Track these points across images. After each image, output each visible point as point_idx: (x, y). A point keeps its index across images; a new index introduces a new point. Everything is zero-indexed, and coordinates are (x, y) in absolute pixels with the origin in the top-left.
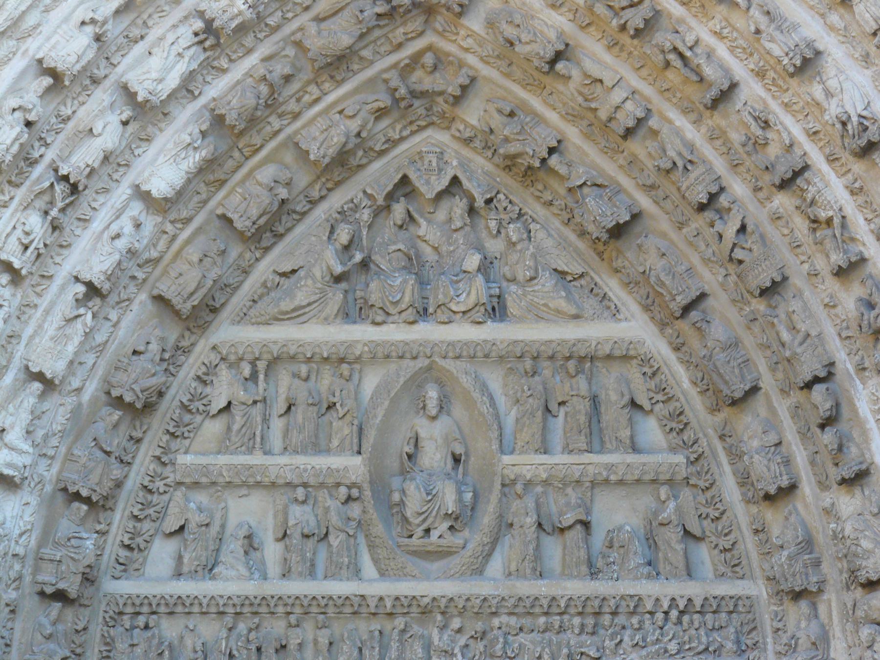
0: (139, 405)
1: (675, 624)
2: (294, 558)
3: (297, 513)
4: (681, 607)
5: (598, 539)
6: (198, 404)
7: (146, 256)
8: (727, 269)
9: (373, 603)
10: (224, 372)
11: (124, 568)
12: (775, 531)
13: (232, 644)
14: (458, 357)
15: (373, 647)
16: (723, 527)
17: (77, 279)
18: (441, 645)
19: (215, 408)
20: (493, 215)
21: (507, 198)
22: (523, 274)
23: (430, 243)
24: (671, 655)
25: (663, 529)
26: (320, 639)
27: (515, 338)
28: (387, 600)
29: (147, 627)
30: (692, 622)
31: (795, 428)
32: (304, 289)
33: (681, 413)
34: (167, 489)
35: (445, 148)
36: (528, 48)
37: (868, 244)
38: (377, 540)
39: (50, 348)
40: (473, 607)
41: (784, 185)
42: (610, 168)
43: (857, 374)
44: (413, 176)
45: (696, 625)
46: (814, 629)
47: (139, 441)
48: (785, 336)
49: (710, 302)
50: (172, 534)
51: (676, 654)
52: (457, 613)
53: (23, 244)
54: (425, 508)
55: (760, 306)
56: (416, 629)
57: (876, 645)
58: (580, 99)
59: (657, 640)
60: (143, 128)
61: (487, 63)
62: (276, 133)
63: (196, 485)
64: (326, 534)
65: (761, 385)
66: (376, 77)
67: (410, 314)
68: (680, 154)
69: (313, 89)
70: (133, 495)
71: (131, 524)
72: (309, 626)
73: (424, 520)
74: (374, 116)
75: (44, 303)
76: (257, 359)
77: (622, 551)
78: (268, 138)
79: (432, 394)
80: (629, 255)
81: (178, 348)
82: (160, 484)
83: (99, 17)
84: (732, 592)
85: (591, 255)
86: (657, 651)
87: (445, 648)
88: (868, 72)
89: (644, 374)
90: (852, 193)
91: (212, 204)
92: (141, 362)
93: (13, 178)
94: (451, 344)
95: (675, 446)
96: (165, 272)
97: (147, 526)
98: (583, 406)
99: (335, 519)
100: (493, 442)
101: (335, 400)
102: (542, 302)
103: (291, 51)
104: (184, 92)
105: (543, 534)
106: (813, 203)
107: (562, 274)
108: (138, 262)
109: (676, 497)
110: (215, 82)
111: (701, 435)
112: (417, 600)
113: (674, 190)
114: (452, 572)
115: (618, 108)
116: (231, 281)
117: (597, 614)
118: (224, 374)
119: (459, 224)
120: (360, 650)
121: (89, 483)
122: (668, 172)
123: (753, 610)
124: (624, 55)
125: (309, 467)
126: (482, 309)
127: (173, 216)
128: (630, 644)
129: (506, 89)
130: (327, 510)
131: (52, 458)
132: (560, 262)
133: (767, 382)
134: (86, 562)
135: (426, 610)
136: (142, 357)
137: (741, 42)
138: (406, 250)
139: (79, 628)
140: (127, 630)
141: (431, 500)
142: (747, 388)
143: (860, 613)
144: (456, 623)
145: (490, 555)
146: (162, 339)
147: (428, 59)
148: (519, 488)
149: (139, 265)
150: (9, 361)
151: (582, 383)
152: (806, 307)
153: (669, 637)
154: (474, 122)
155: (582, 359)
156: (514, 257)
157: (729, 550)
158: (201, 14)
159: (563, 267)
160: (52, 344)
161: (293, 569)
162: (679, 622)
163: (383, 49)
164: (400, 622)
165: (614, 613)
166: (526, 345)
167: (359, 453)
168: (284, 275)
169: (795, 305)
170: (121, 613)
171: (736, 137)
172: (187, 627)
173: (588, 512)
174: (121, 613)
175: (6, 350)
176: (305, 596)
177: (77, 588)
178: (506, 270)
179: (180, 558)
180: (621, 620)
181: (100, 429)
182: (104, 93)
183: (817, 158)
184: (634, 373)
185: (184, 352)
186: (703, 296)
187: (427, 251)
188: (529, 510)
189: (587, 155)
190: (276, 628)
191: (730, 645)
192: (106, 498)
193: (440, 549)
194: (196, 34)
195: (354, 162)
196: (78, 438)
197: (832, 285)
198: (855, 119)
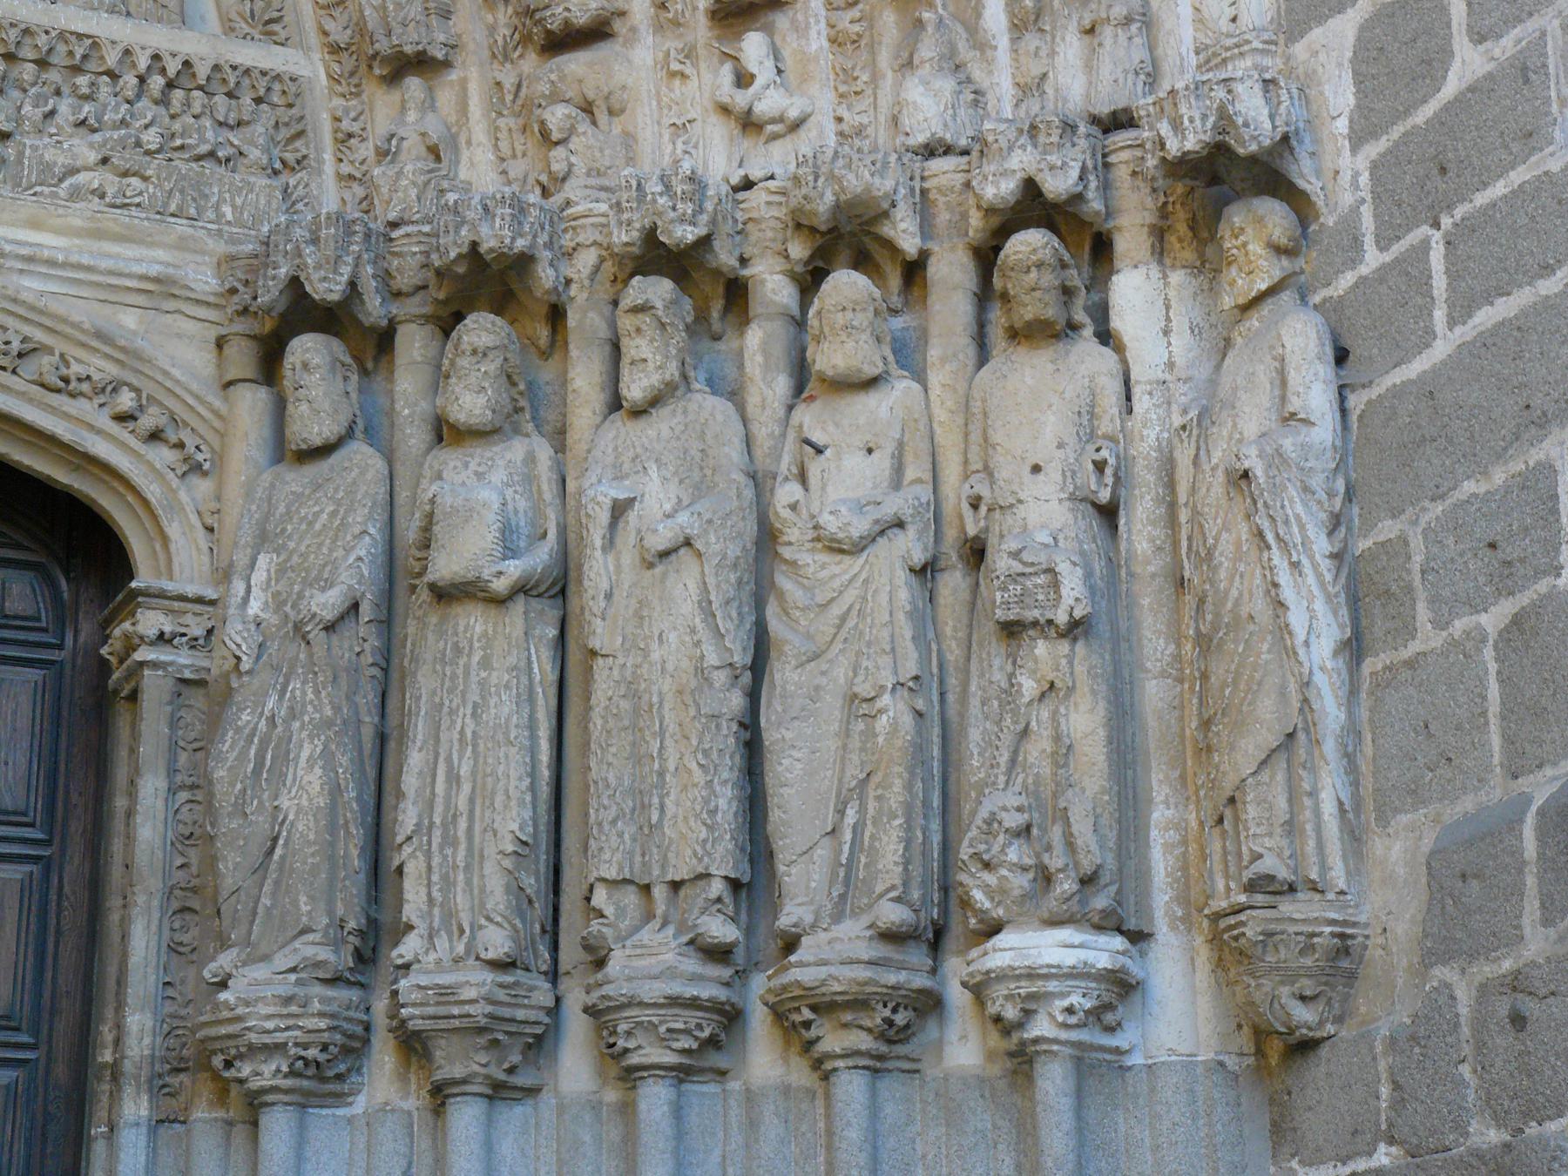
1: (156, 103)
4: (171, 72)
24: (148, 153)
30: (187, 104)
45: (197, 109)
51: (158, 151)
57: (574, 139)
59: (123, 121)
84: (265, 64)
86: (121, 139)
123: (298, 102)
128: (71, 118)
153: (146, 121)
180: (53, 76)
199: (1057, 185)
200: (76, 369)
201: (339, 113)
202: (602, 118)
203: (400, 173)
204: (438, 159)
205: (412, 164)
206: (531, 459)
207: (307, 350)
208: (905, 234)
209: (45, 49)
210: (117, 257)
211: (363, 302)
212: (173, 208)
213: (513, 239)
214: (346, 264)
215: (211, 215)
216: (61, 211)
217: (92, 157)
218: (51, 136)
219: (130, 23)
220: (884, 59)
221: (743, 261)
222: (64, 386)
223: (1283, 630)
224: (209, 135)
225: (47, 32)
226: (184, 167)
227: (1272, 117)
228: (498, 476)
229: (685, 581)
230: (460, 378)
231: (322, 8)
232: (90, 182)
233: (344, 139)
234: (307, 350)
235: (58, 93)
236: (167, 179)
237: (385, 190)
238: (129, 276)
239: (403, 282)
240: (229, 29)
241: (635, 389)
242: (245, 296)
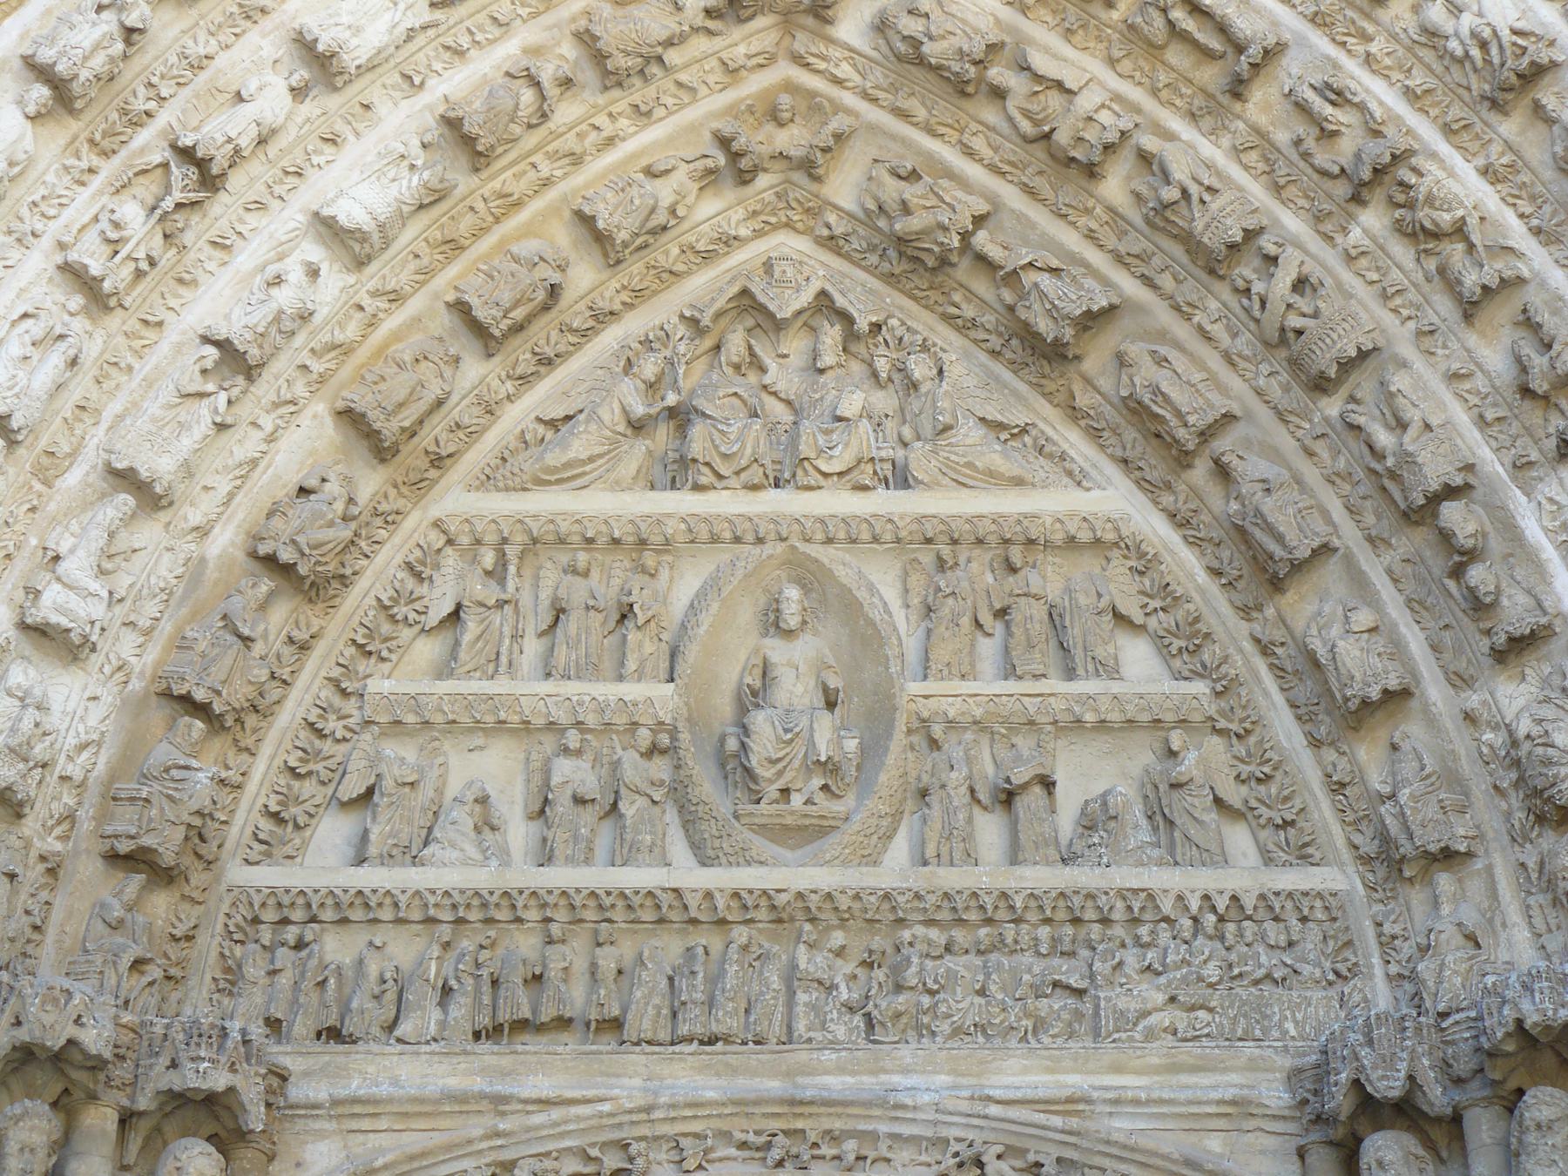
1: (1211, 938)
3: (564, 769)
8: (1271, 365)
10: (451, 562)
11: (265, 849)
12: (1377, 781)
13: (448, 969)
14: (829, 541)
15: (693, 973)
16: (1282, 788)
17: (206, 340)
18: (811, 969)
19: (433, 618)
21: (903, 323)
23: (782, 395)
24: (1211, 986)
25: (1176, 795)
26: (600, 962)
27: (922, 511)
28: (717, 895)
29: (300, 945)
31: (1401, 599)
32: (584, 436)
33: (1197, 620)
34: (348, 735)
35: (806, 259)
37: (1528, 253)
38: (700, 808)
39: (151, 433)
40: (866, 911)
42: (1072, 240)
43: (1514, 479)
47: (304, 647)
51: (1218, 983)
52: (836, 922)
53: (109, 241)
54: (780, 754)
58: (1026, 126)
61: (875, 100)
62: (547, 183)
64: (615, 805)
65: (1336, 542)
66: (701, 125)
70: (290, 735)
73: (780, 774)
74: (696, 186)
75: (144, 368)
76: (505, 541)
77: (1113, 824)
78: (531, 193)
84: (1305, 886)
86: (1184, 979)
87: (819, 975)
89: (1131, 569)
93: (98, 137)
95: (1187, 674)
97: (308, 788)
98: (1039, 611)
100: (892, 663)
101: (631, 599)
102: (963, 461)
104: (397, 78)
105: (977, 810)
106: (1430, 200)
108: (312, 344)
109: (1199, 747)
110: (446, 74)
111: (1231, 651)
112: (770, 898)
113: (1178, 251)
114: (828, 856)
116: (466, 421)
118: (450, 559)
120: (671, 979)
121: (209, 679)
125: (587, 698)
126: (869, 469)
129: (905, 142)
130: (616, 765)
132: (989, 408)
133: (1349, 535)
134: (194, 805)
135: (784, 916)
136: (312, 497)
138: (745, 395)
139: (178, 933)
140: (264, 947)
141: (792, 740)
142: (1315, 544)
145: (889, 836)
146: (347, 480)
149: (312, 350)
151: (1034, 580)
154: (848, 203)
156: (915, 404)
157: (1292, 823)
159: (993, 414)
161: (557, 852)
166: (943, 522)
167: (672, 680)
168: (552, 424)
170: (256, 921)
172: (371, 943)
175: (71, 429)
176: (578, 890)
177: (176, 849)
180: (1118, 931)
182: (264, 36)
185: (387, 522)
186: (1229, 418)
188: (954, 762)
189: (1033, 226)
193: (807, 822)
198: (1505, 34)
201: (1380, 919)
203: (1442, 964)
204: (1478, 946)
205: (1455, 956)
207: (1379, 1149)
209: (1106, 909)
210: (1195, 1087)
211: (1424, 1093)
212: (1240, 1033)
213: (1555, 1010)
214: (1401, 1060)
215: (1275, 1034)
216: (1139, 1053)
217: (1160, 998)
218: (1121, 985)
219: (1177, 871)
224: (1263, 959)
225: (1106, 893)
226: (1243, 994)
230: (1528, 1154)
231: (1349, 824)
232: (1162, 1021)
233: (1387, 943)
234: (1379, 1149)
235: (1123, 945)
236: (1231, 1006)
237: (1430, 983)
238: (1208, 1103)
239: (1463, 1067)
240: (1268, 859)
242: (1315, 1104)
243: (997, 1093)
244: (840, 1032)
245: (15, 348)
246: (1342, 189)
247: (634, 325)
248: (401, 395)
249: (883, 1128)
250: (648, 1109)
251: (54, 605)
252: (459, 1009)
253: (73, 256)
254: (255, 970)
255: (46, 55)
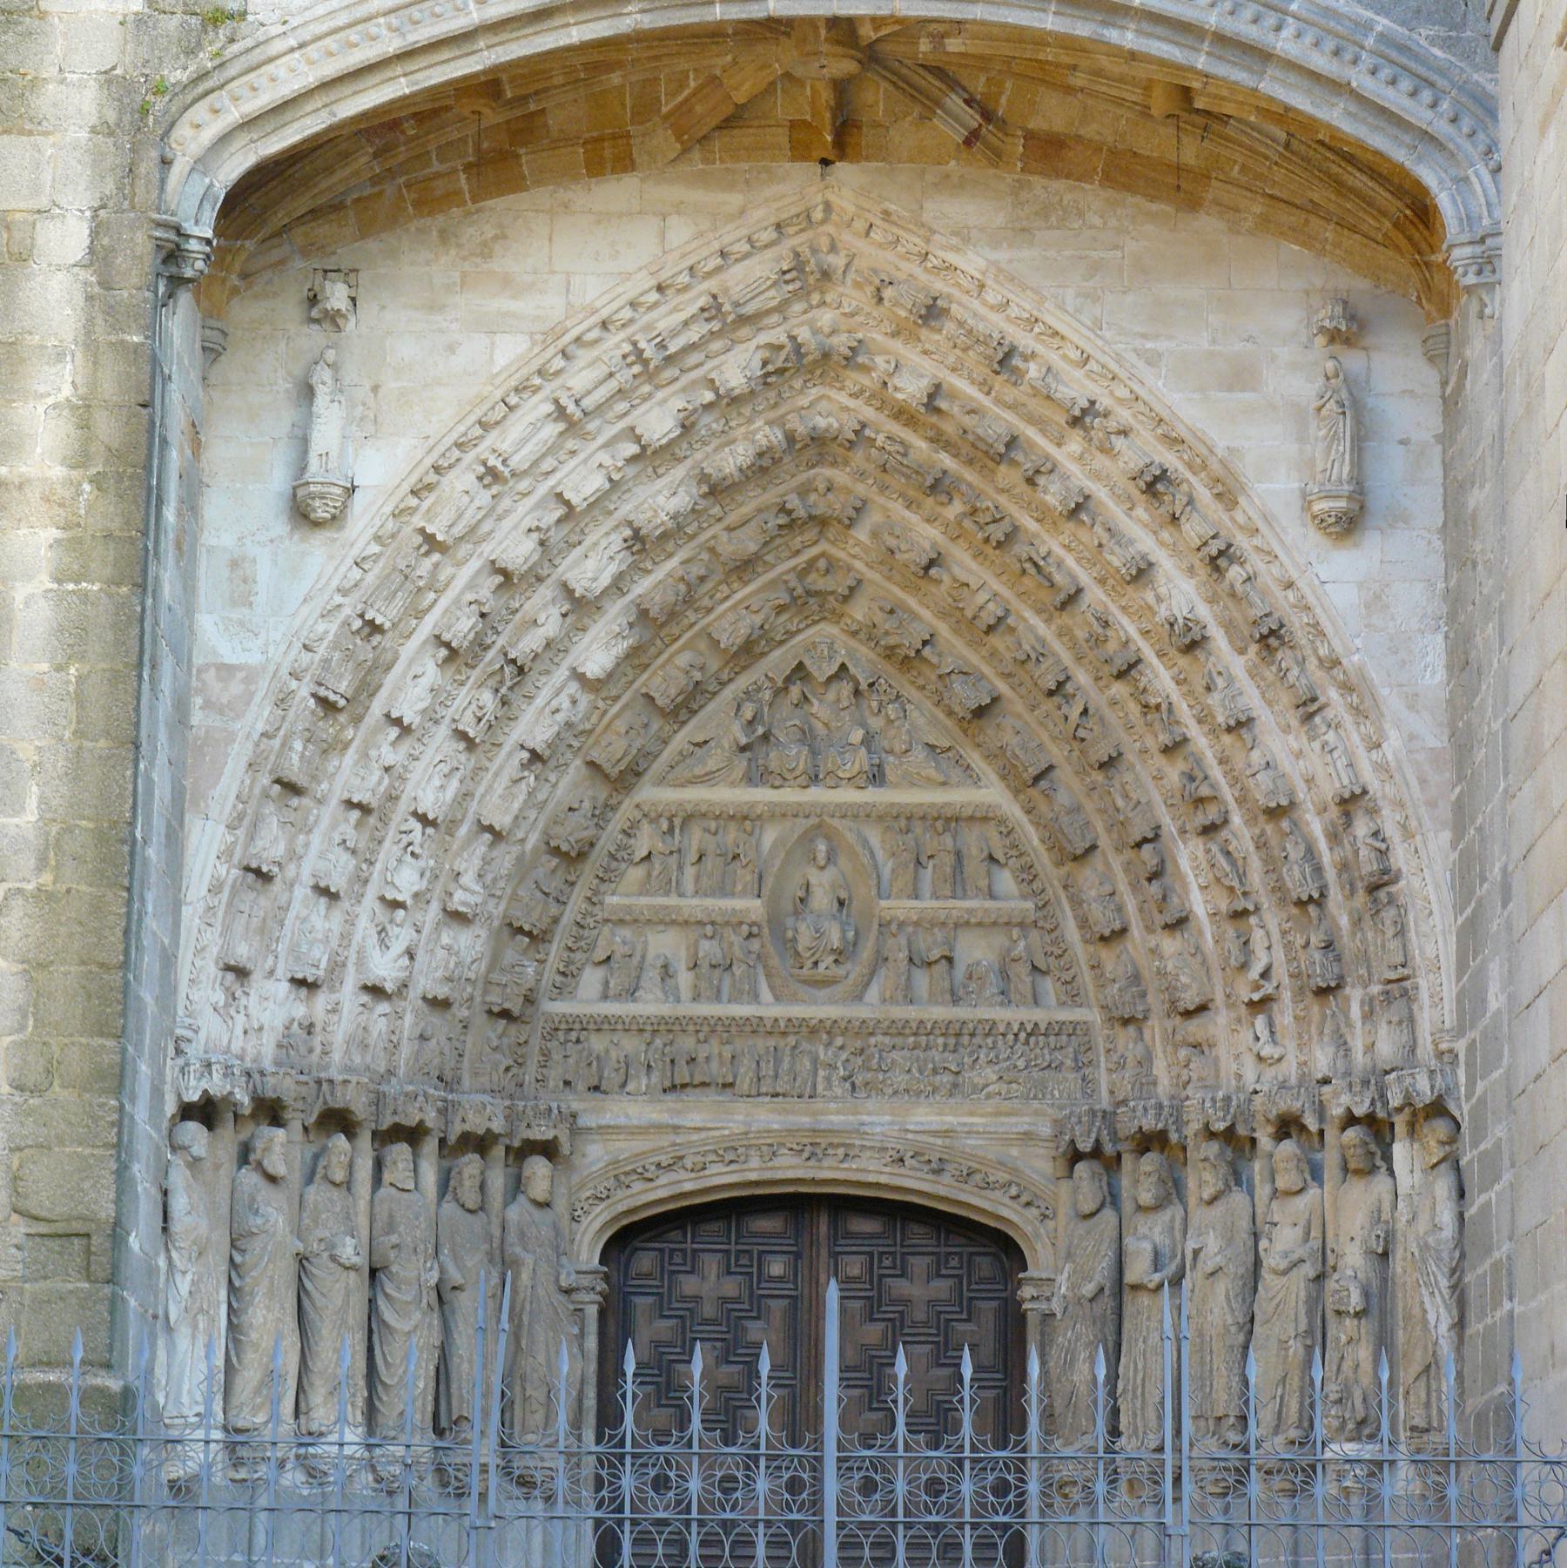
0: (573, 854)
2: (703, 985)
3: (706, 946)
5: (960, 971)
6: (623, 854)
7: (581, 727)
9: (769, 1024)
11: (560, 991)
14: (843, 817)
17: (522, 747)
20: (875, 696)
22: (899, 747)
36: (906, 556)
41: (1121, 675)
42: (974, 659)
44: (807, 662)
46: (1139, 1050)
47: (573, 884)
48: (1120, 803)
49: (1056, 773)
50: (600, 963)
55: (1099, 777)
56: (805, 1046)
60: (580, 619)
62: (692, 625)
63: (622, 922)
67: (803, 780)
68: (1033, 648)
69: (724, 587)
71: (565, 954)
72: (714, 1042)
75: (494, 767)
79: (822, 847)
80: (989, 732)
81: (607, 805)
82: (590, 921)
83: (543, 525)
85: (957, 731)
88: (1193, 582)
90: (1178, 683)
91: (637, 685)
92: (576, 817)
94: (837, 805)
96: (597, 742)
97: (579, 956)
98: (948, 860)
99: (737, 952)
103: (705, 556)
106: (1145, 690)
107: (932, 747)
109: (1025, 937)
115: (981, 608)
117: (958, 1035)
118: (646, 828)
119: (845, 704)
122: (1023, 662)
124: (988, 563)
127: (604, 695)
130: (731, 944)
131: (500, 898)
133: (1104, 842)
134: (528, 986)
137: (1086, 554)
143: (1179, 1037)
144: (839, 1041)
145: (867, 984)
146: (594, 798)
147: (822, 564)
148: (894, 927)
150: (464, 816)
151: (948, 840)
152: (1137, 779)
154: (860, 618)
155: (948, 820)
156: (892, 732)
158: (630, 524)
160: (499, 801)
162: (1027, 1042)
163: (783, 555)
164: (791, 1040)
165: (972, 1035)
168: (697, 745)
169: (1128, 777)
170: (557, 1029)
171: (1081, 634)
173: (951, 950)
174: (557, 1029)
178: (886, 744)
179: (606, 984)
180: (977, 1040)
181: (540, 873)
183: (1148, 653)
184: (992, 832)
186: (1051, 768)
187: (819, 726)
190: (687, 1043)
191: (1069, 1062)
192: (545, 932)
194: (625, 541)
195: (757, 650)
196: (521, 880)
197: (1160, 761)
198: (1181, 621)
199: (1359, 1111)
200: (991, 1179)
202: (1207, 1051)
206: (1172, 1220)
208: (1311, 1123)
217: (995, 1077)
220: (1313, 1029)
221: (1254, 1130)
222: (987, 1186)
223: (1425, 1321)
227: (1432, 1087)
228: (1157, 1230)
229: (1222, 1286)
241: (1207, 1194)
243: (911, 1127)
244: (839, 1091)
245: (437, 782)
246: (1106, 670)
247: (743, 682)
248: (619, 756)
249: (857, 1142)
250: (746, 1133)
251: (459, 900)
252: (655, 1078)
253: (461, 727)
254: (556, 1056)
255: (446, 637)
